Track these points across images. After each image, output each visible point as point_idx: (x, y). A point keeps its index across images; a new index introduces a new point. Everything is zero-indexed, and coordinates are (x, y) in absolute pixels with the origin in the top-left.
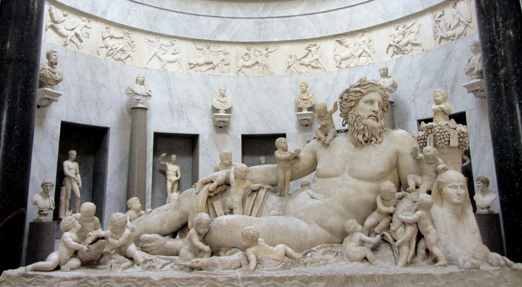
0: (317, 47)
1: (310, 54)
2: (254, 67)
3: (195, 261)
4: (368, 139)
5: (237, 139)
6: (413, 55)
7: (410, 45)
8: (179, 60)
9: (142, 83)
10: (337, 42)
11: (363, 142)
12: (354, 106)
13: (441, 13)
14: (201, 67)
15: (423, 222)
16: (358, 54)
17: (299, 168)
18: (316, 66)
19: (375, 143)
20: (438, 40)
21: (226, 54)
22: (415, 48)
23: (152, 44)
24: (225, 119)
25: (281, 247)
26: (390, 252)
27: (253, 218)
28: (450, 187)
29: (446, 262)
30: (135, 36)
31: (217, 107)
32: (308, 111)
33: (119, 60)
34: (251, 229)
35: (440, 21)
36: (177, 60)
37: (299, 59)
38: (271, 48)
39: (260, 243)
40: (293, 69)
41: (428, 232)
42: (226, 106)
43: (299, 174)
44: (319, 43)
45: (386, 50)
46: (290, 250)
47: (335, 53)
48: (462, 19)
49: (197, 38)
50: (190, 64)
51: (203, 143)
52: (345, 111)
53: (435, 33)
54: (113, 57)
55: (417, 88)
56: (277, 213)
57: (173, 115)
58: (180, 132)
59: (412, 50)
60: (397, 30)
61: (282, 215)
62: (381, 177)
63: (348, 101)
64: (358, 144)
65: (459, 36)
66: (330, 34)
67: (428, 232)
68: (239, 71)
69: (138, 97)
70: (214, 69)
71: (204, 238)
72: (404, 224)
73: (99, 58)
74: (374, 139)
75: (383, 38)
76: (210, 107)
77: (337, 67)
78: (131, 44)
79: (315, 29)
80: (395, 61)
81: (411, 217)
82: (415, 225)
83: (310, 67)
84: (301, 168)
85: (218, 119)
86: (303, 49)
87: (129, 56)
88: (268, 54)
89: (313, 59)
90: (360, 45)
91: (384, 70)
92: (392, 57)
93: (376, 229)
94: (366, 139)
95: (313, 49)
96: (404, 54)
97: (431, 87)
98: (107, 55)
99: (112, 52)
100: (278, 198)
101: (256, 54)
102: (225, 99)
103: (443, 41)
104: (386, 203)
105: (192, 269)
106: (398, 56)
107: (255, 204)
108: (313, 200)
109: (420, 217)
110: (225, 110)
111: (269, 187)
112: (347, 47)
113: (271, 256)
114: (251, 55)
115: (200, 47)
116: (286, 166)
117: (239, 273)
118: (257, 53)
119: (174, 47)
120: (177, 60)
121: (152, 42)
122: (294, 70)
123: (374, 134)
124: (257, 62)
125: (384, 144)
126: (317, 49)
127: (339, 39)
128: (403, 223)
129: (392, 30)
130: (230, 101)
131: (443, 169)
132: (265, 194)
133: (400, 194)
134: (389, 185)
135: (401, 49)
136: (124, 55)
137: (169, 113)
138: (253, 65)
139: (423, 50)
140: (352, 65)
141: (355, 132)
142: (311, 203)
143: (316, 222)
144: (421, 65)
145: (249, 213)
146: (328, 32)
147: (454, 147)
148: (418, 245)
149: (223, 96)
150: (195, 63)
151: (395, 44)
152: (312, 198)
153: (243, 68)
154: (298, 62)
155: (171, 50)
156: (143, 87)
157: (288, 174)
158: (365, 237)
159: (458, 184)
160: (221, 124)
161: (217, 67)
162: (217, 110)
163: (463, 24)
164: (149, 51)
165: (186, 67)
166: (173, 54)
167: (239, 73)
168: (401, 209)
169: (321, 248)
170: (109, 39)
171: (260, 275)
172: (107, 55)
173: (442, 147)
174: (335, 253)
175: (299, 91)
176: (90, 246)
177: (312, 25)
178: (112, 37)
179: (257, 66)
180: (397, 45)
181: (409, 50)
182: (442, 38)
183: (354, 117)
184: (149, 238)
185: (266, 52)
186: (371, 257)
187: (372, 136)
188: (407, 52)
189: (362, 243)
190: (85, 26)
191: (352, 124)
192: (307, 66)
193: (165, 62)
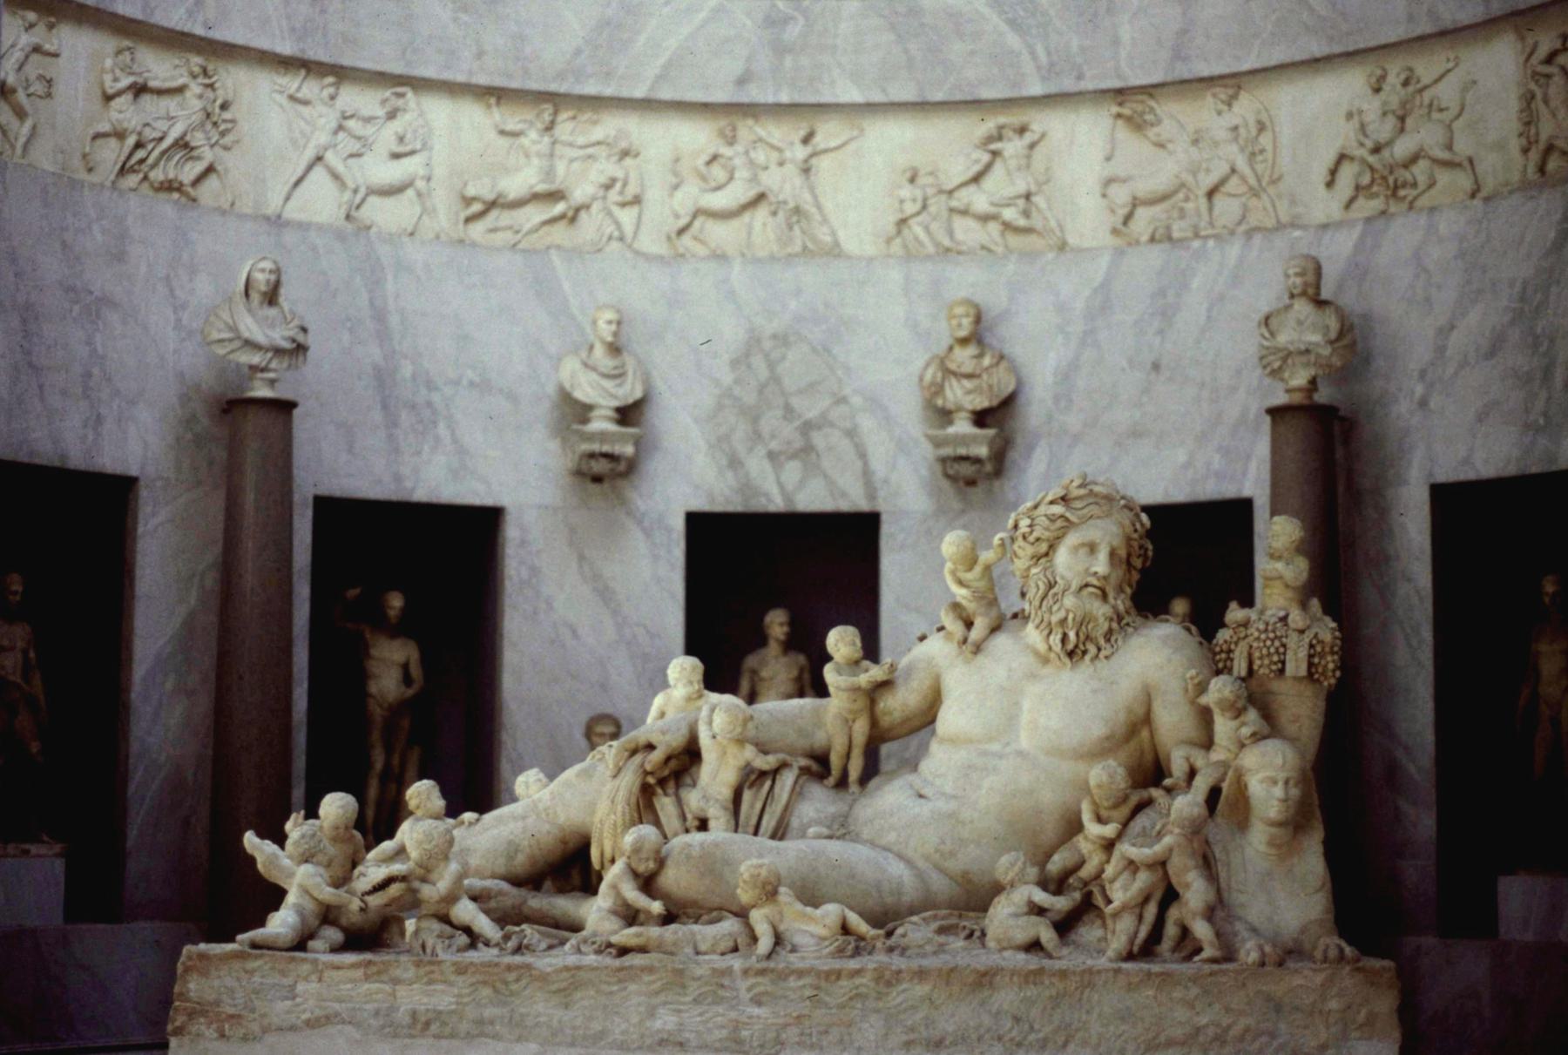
0: (1028, 138)
1: (998, 168)
2: (746, 217)
3: (628, 935)
4: (1076, 646)
5: (669, 530)
6: (1432, 210)
7: (1423, 164)
12: (1047, 554)
16: (1208, 181)
18: (1022, 222)
20: (1534, 156)
21: (625, 154)
23: (305, 110)
25: (831, 911)
27: (763, 841)
29: (1216, 953)
30: (236, 79)
31: (584, 393)
33: (169, 186)
34: (761, 866)
38: (830, 132)
40: (919, 231)
41: (1188, 886)
45: (1320, 172)
46: (854, 920)
49: (498, 82)
50: (468, 201)
53: (1528, 124)
54: (146, 178)
55: (1441, 350)
56: (825, 831)
57: (395, 424)
59: (1432, 185)
60: (1377, 90)
61: (838, 838)
66: (1088, 85)
67: (1188, 886)
69: (256, 359)
70: (573, 220)
71: (647, 883)
72: (1132, 866)
73: (93, 186)
74: (1092, 649)
76: (551, 389)
77: (1115, 232)
78: (218, 117)
79: (1026, 57)
80: (1359, 229)
83: (994, 228)
87: (210, 170)
88: (814, 161)
89: (1010, 191)
90: (1216, 144)
94: (1070, 647)
98: (123, 171)
99: (140, 154)
100: (832, 793)
105: (623, 951)
106: (1376, 204)
108: (923, 801)
110: (619, 410)
111: (804, 762)
112: (1161, 146)
114: (738, 161)
115: (511, 126)
117: (736, 963)
119: (397, 126)
121: (306, 103)
126: (1032, 146)
132: (796, 782)
136: (189, 165)
142: (917, 810)
144: (1461, 255)
145: (751, 829)
146: (1080, 77)
150: (490, 197)
151: (1363, 152)
152: (921, 796)
155: (386, 136)
158: (1040, 897)
160: (600, 466)
161: (583, 215)
162: (583, 412)
164: (294, 142)
165: (445, 216)
166: (396, 156)
169: (935, 917)
170: (129, 97)
171: (781, 966)
172: (123, 171)
174: (967, 932)
176: (369, 899)
177: (1013, 40)
178: (139, 90)
179: (762, 213)
180: (1371, 159)
181: (1422, 187)
184: (484, 889)
185: (800, 152)
187: (1088, 638)
189: (1039, 911)
190: (37, 49)
192: (985, 218)
193: (363, 191)
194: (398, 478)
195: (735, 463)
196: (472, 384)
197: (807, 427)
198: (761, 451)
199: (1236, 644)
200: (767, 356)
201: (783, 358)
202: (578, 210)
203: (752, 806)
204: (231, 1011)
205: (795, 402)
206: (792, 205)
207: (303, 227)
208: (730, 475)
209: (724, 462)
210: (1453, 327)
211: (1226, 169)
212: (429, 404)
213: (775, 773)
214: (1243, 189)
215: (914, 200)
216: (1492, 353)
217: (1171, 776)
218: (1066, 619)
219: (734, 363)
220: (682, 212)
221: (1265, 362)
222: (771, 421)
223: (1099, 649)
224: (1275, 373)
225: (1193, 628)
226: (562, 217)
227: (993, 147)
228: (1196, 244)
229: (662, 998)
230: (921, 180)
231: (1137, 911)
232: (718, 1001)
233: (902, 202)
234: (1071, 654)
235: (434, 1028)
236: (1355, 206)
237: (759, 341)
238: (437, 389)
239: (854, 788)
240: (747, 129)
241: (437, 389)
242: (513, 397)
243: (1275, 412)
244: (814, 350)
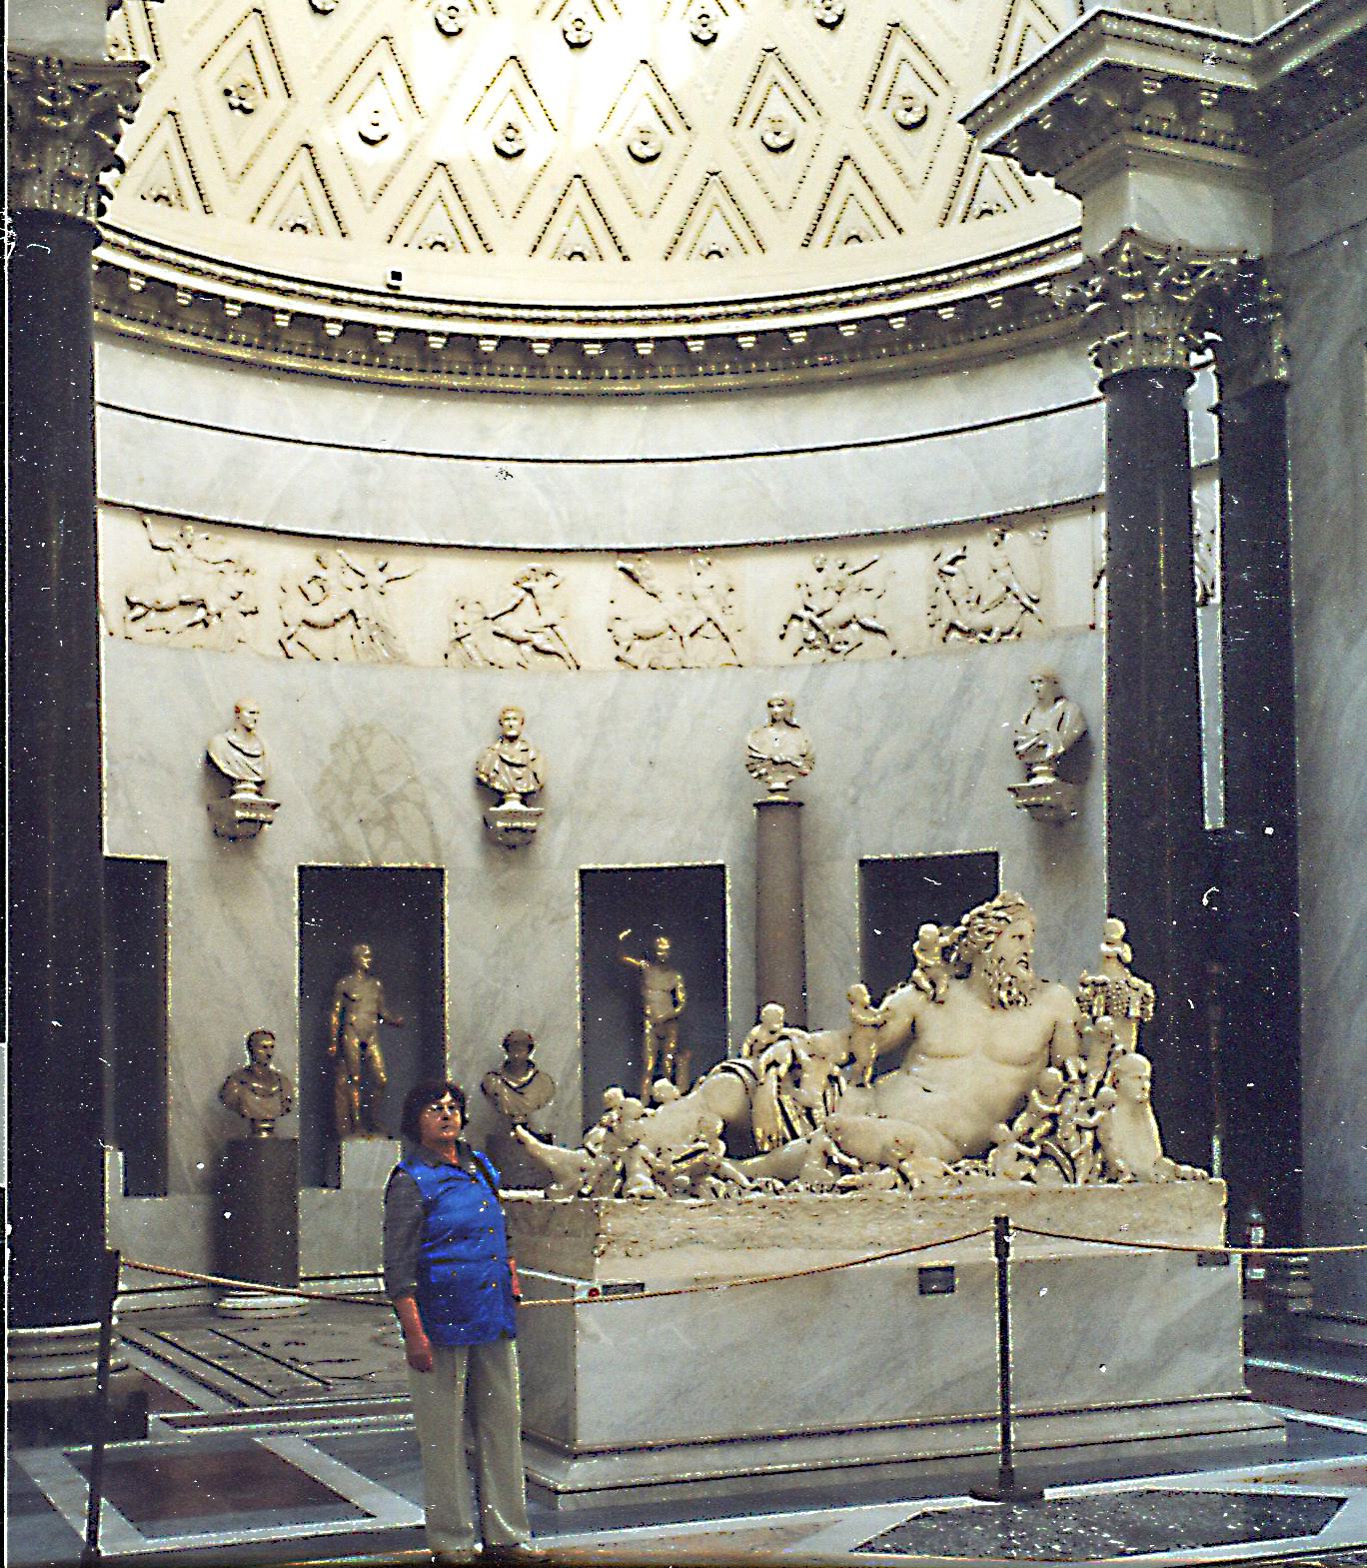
0: (552, 580)
6: (863, 662)
7: (855, 627)
10: (622, 575)
13: (959, 552)
14: (165, 615)
22: (869, 639)
28: (1133, 1078)
32: (523, 802)
35: (952, 575)
37: (491, 615)
38: (399, 563)
44: (563, 567)
47: (616, 610)
48: (1016, 588)
50: (132, 605)
55: (868, 763)
60: (820, 570)
63: (985, 931)
65: (1003, 634)
74: (1022, 999)
75: (772, 586)
80: (807, 671)
85: (239, 814)
86: (509, 585)
93: (1033, 1137)
95: (542, 586)
97: (908, 767)
101: (343, 580)
103: (955, 634)
118: (355, 581)
122: (474, 653)
124: (352, 612)
127: (629, 566)
129: (800, 564)
135: (827, 636)
140: (669, 660)
143: (938, 1127)
154: (491, 626)
163: (1015, 601)
175: (490, 726)
180: (818, 621)
182: (953, 626)
185: (382, 578)
188: (845, 648)
195: (335, 827)
197: (389, 801)
201: (370, 744)
204: (633, 1239)
205: (380, 780)
208: (331, 836)
209: (326, 825)
210: (877, 748)
216: (908, 767)
219: (334, 747)
222: (361, 795)
227: (527, 585)
228: (683, 671)
229: (869, 1218)
232: (901, 1216)
235: (747, 1244)
238: (117, 762)
240: (334, 556)
241: (117, 762)
242: (170, 771)
244: (392, 737)
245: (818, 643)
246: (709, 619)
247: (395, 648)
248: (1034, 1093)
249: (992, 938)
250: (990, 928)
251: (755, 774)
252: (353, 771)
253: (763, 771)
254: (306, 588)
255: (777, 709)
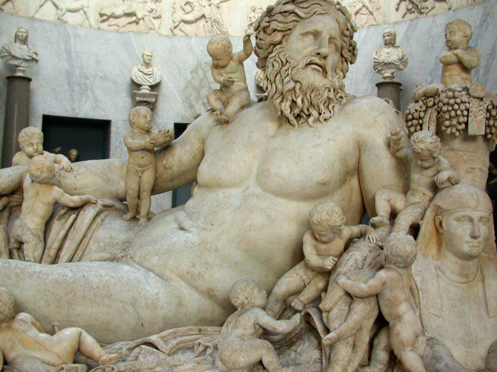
2: (198, 23)
4: (302, 111)
6: (434, 15)
8: (85, 9)
9: (24, 41)
11: (291, 118)
12: (280, 43)
15: (387, 294)
16: (356, 10)
17: (170, 168)
19: (318, 120)
24: (149, 100)
26: (316, 354)
28: (458, 220)
31: (139, 81)
36: (82, 9)
39: (16, 325)
41: (399, 318)
42: (151, 80)
43: (172, 180)
45: (394, 6)
50: (102, 15)
51: (117, 133)
52: (263, 54)
57: (73, 91)
58: (82, 115)
59: (433, 8)
62: (321, 192)
63: (269, 31)
64: (283, 120)
68: (175, 28)
69: (16, 62)
72: (350, 297)
74: (315, 113)
76: (128, 80)
80: (408, 23)
81: (363, 285)
82: (373, 301)
84: (175, 169)
85: (138, 99)
88: (221, 5)
91: (390, 35)
92: (403, 17)
94: (297, 111)
96: (421, 13)
100: (125, 224)
102: (151, 69)
104: (323, 247)
106: (413, 16)
107: (70, 235)
108: (182, 232)
109: (384, 284)
110: (150, 86)
113: (37, 354)
116: (142, 162)
120: (82, 9)
123: (315, 102)
124: (203, 16)
125: (332, 124)
128: (348, 294)
130: (158, 73)
131: (449, 180)
133: (356, 229)
134: (331, 212)
135: (417, 6)
137: (66, 88)
138: (197, 20)
139: (450, 9)
141: (277, 95)
147: (474, 138)
148: (376, 341)
149: (148, 65)
152: (182, 229)
153: (183, 23)
156: (25, 47)
157: (148, 178)
159: (476, 215)
161: (141, 21)
162: (138, 86)
167: (176, 31)
168: (351, 262)
173: (453, 135)
179: (202, 22)
181: (430, 8)
183: (276, 65)
186: (271, 362)
187: (311, 104)
188: (427, 11)
191: (272, 79)
193: (64, 10)
194: (73, 109)
195: (191, 106)
196: (101, 78)
198: (200, 102)
199: (425, 111)
200: (203, 70)
202: (139, 20)
203: (58, 234)
206: (213, 19)
207: (42, 21)
208: (189, 110)
209: (188, 106)
211: (361, 5)
212: (85, 84)
213: (76, 209)
214: (367, 12)
215: (254, 17)
217: (375, 215)
218: (294, 88)
219: (192, 72)
220: (175, 21)
221: (376, 67)
223: (320, 114)
224: (379, 72)
225: (391, 102)
226: (135, 21)
230: (257, 11)
231: (351, 340)
233: (250, 18)
234: (298, 117)
236: (406, 16)
237: (201, 65)
238: (88, 79)
239: (142, 221)
241: (88, 79)
243: (379, 85)
245: (413, 10)
246: (364, 6)
247: (223, 30)
248: (308, 240)
249: (278, 37)
250: (274, 25)
251: (377, 71)
252: (201, 82)
253: (380, 68)
254: (184, 7)
255: (387, 38)
